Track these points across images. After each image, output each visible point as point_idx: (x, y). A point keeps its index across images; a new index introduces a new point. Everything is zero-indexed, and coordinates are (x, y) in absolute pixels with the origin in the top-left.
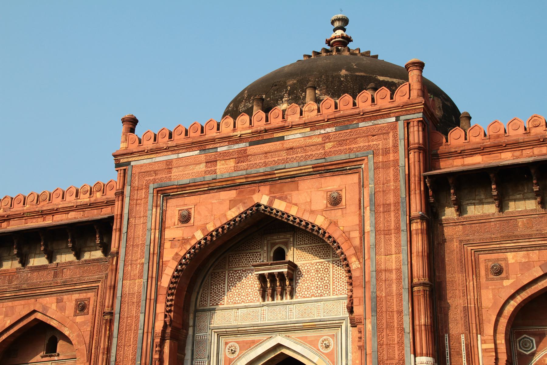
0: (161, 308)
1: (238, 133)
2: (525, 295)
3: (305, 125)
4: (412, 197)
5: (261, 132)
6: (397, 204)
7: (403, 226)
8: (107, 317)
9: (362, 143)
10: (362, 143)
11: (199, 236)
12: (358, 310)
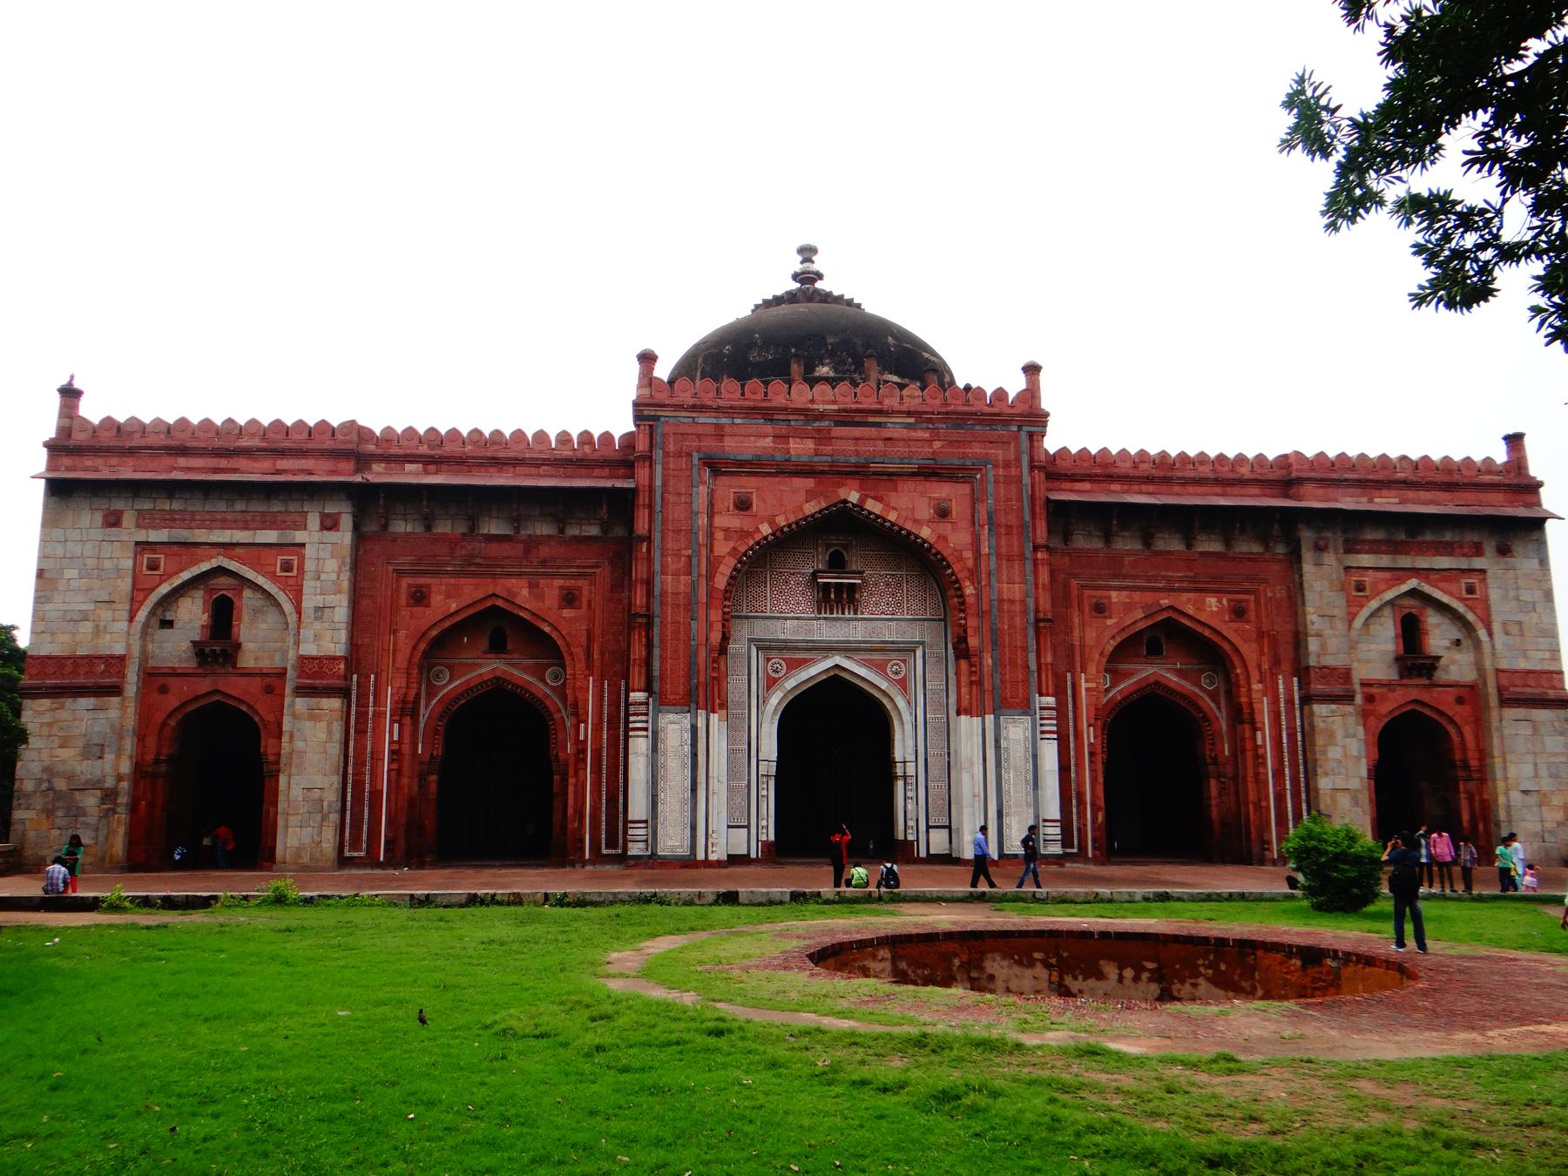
0: (716, 615)
1: (821, 407)
2: (1125, 635)
3: (909, 414)
4: (1038, 523)
5: (851, 411)
6: (1022, 526)
7: (1028, 554)
8: (644, 620)
9: (977, 449)
10: (977, 449)
11: (766, 529)
12: (973, 642)
